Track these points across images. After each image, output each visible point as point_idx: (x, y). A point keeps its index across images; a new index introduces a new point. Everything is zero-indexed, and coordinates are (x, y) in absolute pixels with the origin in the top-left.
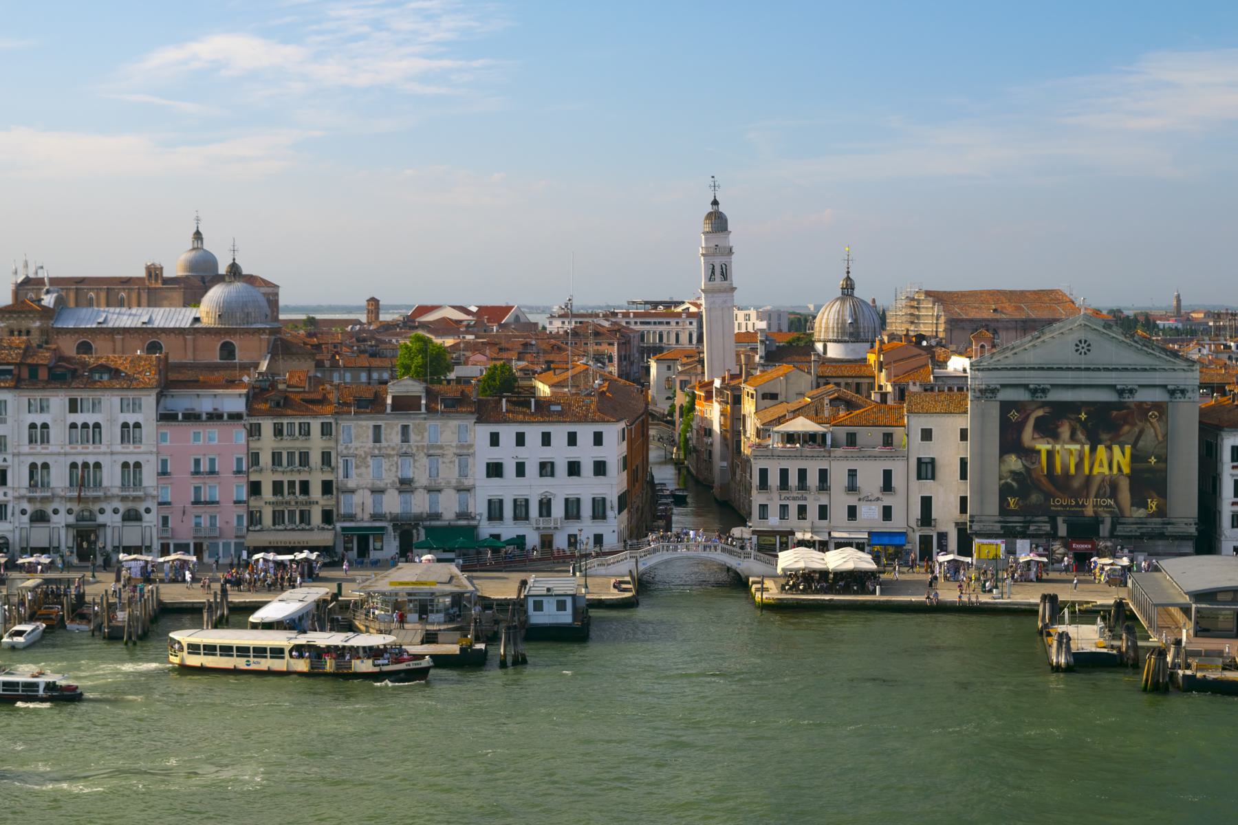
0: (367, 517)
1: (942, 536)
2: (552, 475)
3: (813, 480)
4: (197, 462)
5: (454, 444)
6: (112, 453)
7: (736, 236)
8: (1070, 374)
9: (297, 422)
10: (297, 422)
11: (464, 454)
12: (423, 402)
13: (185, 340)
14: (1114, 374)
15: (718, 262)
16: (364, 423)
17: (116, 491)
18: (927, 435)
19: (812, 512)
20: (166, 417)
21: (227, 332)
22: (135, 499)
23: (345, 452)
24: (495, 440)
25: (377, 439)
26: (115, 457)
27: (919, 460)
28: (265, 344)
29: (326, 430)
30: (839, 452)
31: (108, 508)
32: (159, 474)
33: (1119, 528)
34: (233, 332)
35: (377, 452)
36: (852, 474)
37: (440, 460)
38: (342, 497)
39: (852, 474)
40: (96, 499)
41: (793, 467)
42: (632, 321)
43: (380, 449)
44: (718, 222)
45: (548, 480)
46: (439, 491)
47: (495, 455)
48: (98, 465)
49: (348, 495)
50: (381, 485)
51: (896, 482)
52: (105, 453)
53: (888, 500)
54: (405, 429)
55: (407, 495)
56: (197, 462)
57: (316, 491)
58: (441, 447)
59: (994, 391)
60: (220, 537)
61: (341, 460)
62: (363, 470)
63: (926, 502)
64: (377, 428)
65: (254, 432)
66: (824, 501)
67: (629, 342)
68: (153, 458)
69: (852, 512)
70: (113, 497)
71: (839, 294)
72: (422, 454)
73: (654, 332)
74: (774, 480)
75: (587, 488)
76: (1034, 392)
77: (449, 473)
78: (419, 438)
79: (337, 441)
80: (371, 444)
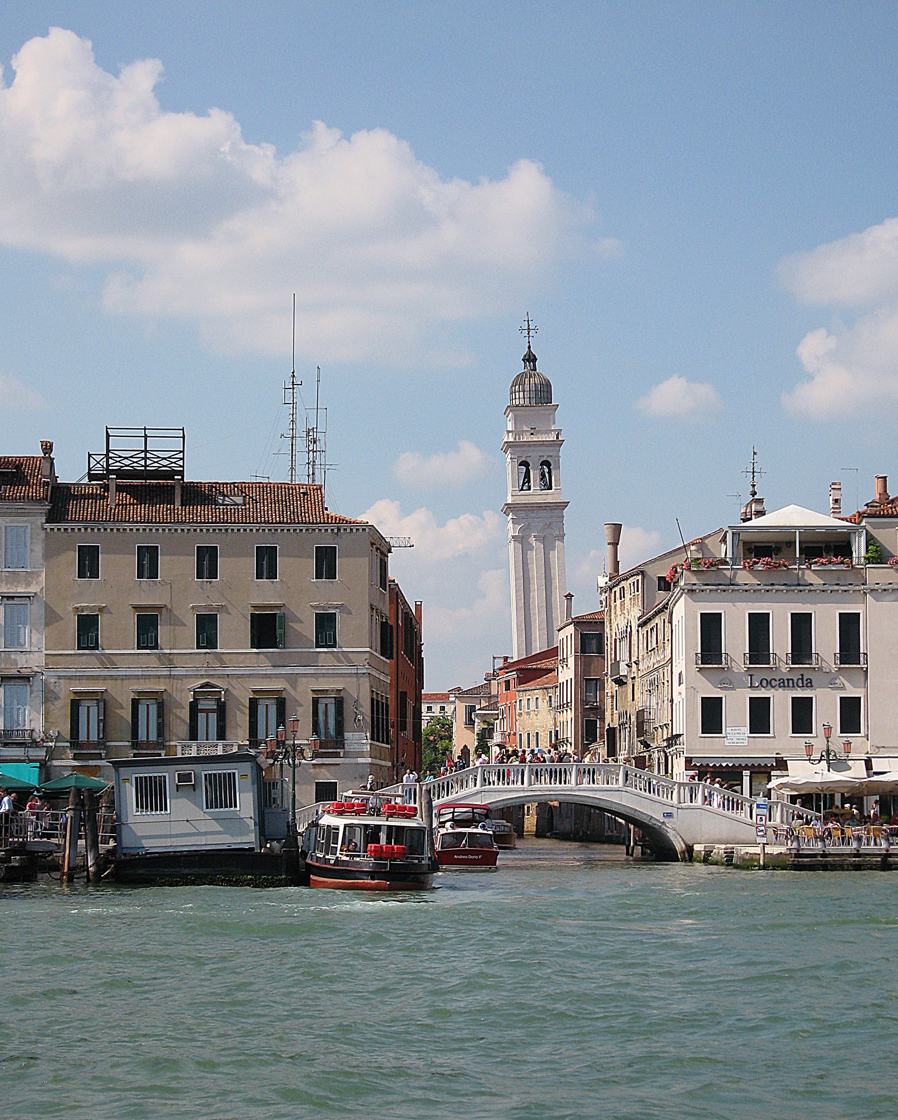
3: (826, 640)
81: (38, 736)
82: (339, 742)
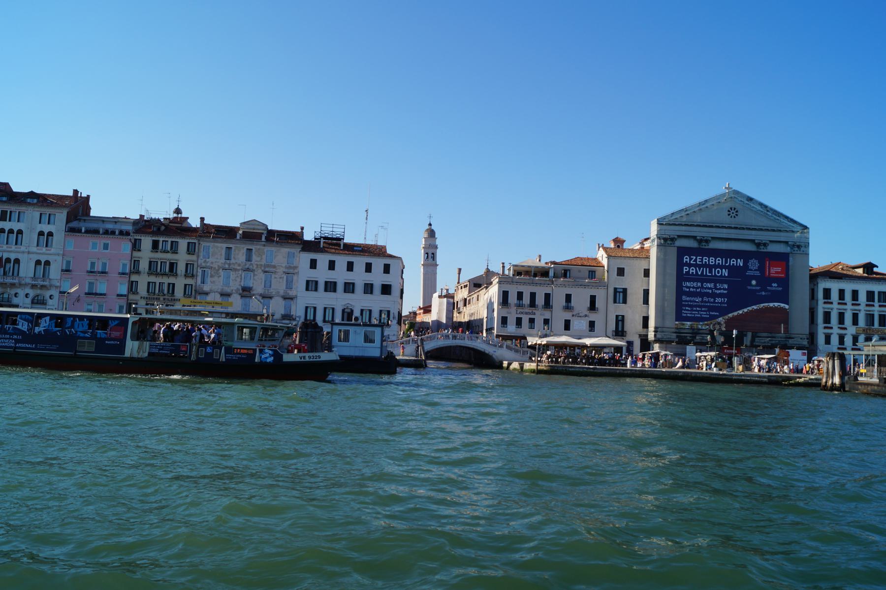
1: (630, 344)
2: (353, 292)
3: (540, 300)
4: (93, 264)
5: (284, 265)
6: (29, 253)
8: (725, 230)
9: (170, 240)
11: (291, 272)
14: (754, 232)
17: (28, 281)
20: (72, 230)
22: (43, 287)
23: (203, 264)
24: (313, 264)
25: (228, 258)
26: (31, 256)
27: (615, 289)
31: (21, 292)
32: (62, 270)
33: (757, 339)
35: (227, 266)
36: (568, 298)
37: (273, 276)
39: (568, 298)
40: (13, 285)
41: (527, 291)
43: (229, 264)
44: (431, 233)
45: (349, 296)
46: (271, 298)
47: (313, 275)
48: (17, 261)
49: (203, 296)
50: (228, 290)
52: (23, 252)
53: (593, 317)
55: (248, 299)
56: (93, 264)
58: (274, 267)
59: (673, 240)
61: (200, 271)
62: (215, 279)
65: (136, 246)
66: (547, 316)
68: (59, 258)
69: (567, 325)
70: (26, 285)
72: (260, 271)
76: (700, 241)
77: (278, 285)
78: (258, 259)
79: (198, 257)
80: (223, 261)
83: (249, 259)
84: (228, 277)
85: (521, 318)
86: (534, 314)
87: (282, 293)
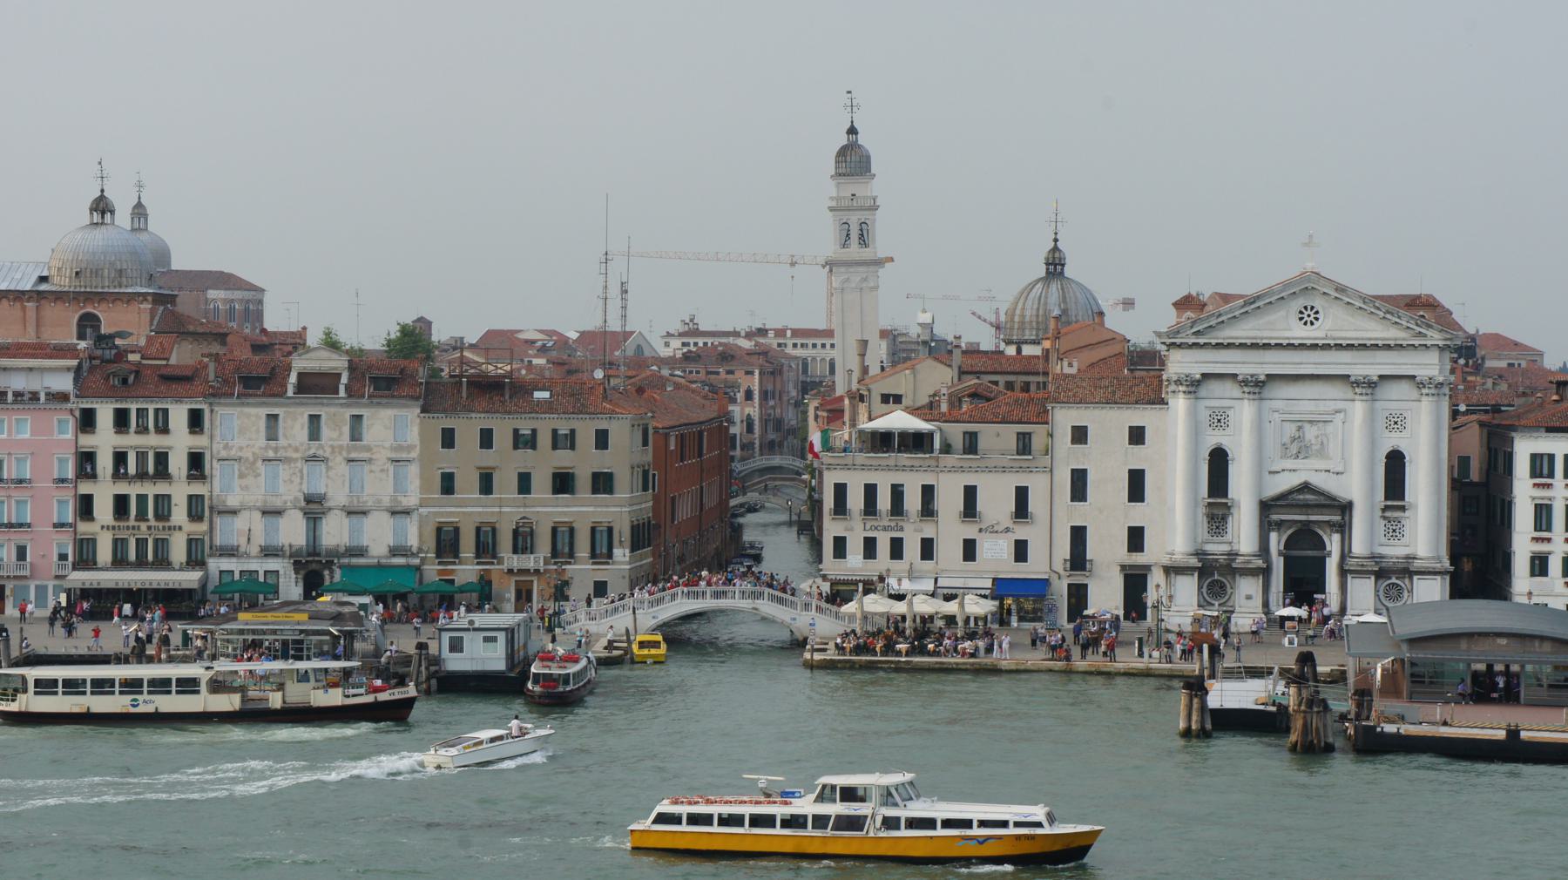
0: (254, 550)
3: (913, 502)
5: (387, 444)
7: (882, 184)
9: (151, 407)
10: (151, 407)
12: (344, 379)
13: (24, 309)
15: (854, 219)
16: (252, 411)
18: (1080, 435)
19: (912, 549)
21: (89, 297)
23: (224, 454)
25: (272, 435)
28: (146, 317)
29: (196, 421)
30: (950, 460)
34: (102, 297)
35: (271, 454)
36: (970, 493)
37: (367, 468)
38: (218, 520)
39: (970, 493)
42: (790, 343)
43: (276, 450)
44: (853, 160)
46: (364, 513)
49: (228, 519)
50: (277, 503)
51: (1035, 504)
53: (1021, 532)
54: (315, 419)
57: (179, 515)
60: (32, 577)
62: (250, 480)
63: (1078, 535)
64: (272, 418)
67: (781, 372)
71: (1043, 274)
72: (339, 459)
73: (823, 360)
74: (855, 500)
75: (583, 509)
78: (335, 435)
79: (211, 437)
80: (262, 442)
81: (415, 550)
82: (610, 555)
83: (314, 434)
84: (276, 476)
85: (874, 539)
86: (902, 529)
87: (386, 502)
